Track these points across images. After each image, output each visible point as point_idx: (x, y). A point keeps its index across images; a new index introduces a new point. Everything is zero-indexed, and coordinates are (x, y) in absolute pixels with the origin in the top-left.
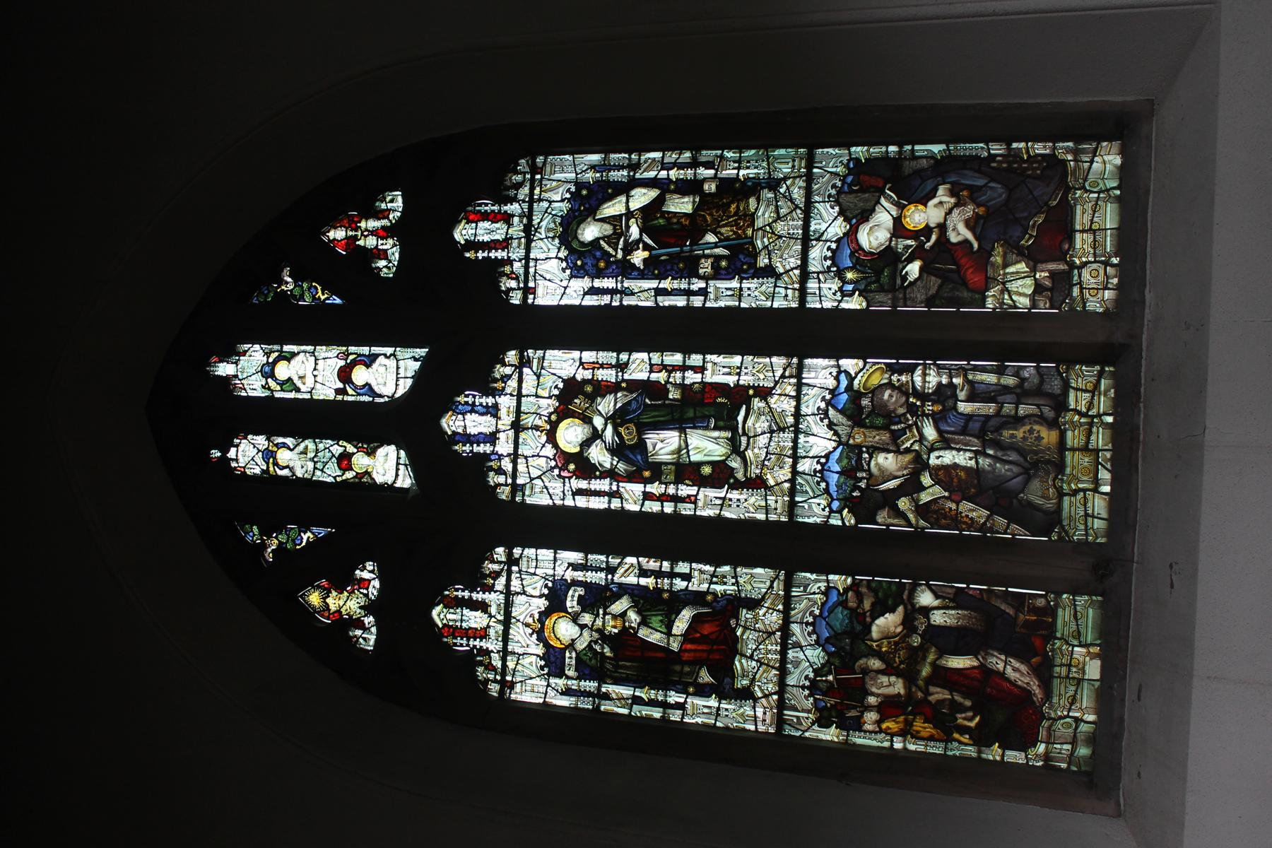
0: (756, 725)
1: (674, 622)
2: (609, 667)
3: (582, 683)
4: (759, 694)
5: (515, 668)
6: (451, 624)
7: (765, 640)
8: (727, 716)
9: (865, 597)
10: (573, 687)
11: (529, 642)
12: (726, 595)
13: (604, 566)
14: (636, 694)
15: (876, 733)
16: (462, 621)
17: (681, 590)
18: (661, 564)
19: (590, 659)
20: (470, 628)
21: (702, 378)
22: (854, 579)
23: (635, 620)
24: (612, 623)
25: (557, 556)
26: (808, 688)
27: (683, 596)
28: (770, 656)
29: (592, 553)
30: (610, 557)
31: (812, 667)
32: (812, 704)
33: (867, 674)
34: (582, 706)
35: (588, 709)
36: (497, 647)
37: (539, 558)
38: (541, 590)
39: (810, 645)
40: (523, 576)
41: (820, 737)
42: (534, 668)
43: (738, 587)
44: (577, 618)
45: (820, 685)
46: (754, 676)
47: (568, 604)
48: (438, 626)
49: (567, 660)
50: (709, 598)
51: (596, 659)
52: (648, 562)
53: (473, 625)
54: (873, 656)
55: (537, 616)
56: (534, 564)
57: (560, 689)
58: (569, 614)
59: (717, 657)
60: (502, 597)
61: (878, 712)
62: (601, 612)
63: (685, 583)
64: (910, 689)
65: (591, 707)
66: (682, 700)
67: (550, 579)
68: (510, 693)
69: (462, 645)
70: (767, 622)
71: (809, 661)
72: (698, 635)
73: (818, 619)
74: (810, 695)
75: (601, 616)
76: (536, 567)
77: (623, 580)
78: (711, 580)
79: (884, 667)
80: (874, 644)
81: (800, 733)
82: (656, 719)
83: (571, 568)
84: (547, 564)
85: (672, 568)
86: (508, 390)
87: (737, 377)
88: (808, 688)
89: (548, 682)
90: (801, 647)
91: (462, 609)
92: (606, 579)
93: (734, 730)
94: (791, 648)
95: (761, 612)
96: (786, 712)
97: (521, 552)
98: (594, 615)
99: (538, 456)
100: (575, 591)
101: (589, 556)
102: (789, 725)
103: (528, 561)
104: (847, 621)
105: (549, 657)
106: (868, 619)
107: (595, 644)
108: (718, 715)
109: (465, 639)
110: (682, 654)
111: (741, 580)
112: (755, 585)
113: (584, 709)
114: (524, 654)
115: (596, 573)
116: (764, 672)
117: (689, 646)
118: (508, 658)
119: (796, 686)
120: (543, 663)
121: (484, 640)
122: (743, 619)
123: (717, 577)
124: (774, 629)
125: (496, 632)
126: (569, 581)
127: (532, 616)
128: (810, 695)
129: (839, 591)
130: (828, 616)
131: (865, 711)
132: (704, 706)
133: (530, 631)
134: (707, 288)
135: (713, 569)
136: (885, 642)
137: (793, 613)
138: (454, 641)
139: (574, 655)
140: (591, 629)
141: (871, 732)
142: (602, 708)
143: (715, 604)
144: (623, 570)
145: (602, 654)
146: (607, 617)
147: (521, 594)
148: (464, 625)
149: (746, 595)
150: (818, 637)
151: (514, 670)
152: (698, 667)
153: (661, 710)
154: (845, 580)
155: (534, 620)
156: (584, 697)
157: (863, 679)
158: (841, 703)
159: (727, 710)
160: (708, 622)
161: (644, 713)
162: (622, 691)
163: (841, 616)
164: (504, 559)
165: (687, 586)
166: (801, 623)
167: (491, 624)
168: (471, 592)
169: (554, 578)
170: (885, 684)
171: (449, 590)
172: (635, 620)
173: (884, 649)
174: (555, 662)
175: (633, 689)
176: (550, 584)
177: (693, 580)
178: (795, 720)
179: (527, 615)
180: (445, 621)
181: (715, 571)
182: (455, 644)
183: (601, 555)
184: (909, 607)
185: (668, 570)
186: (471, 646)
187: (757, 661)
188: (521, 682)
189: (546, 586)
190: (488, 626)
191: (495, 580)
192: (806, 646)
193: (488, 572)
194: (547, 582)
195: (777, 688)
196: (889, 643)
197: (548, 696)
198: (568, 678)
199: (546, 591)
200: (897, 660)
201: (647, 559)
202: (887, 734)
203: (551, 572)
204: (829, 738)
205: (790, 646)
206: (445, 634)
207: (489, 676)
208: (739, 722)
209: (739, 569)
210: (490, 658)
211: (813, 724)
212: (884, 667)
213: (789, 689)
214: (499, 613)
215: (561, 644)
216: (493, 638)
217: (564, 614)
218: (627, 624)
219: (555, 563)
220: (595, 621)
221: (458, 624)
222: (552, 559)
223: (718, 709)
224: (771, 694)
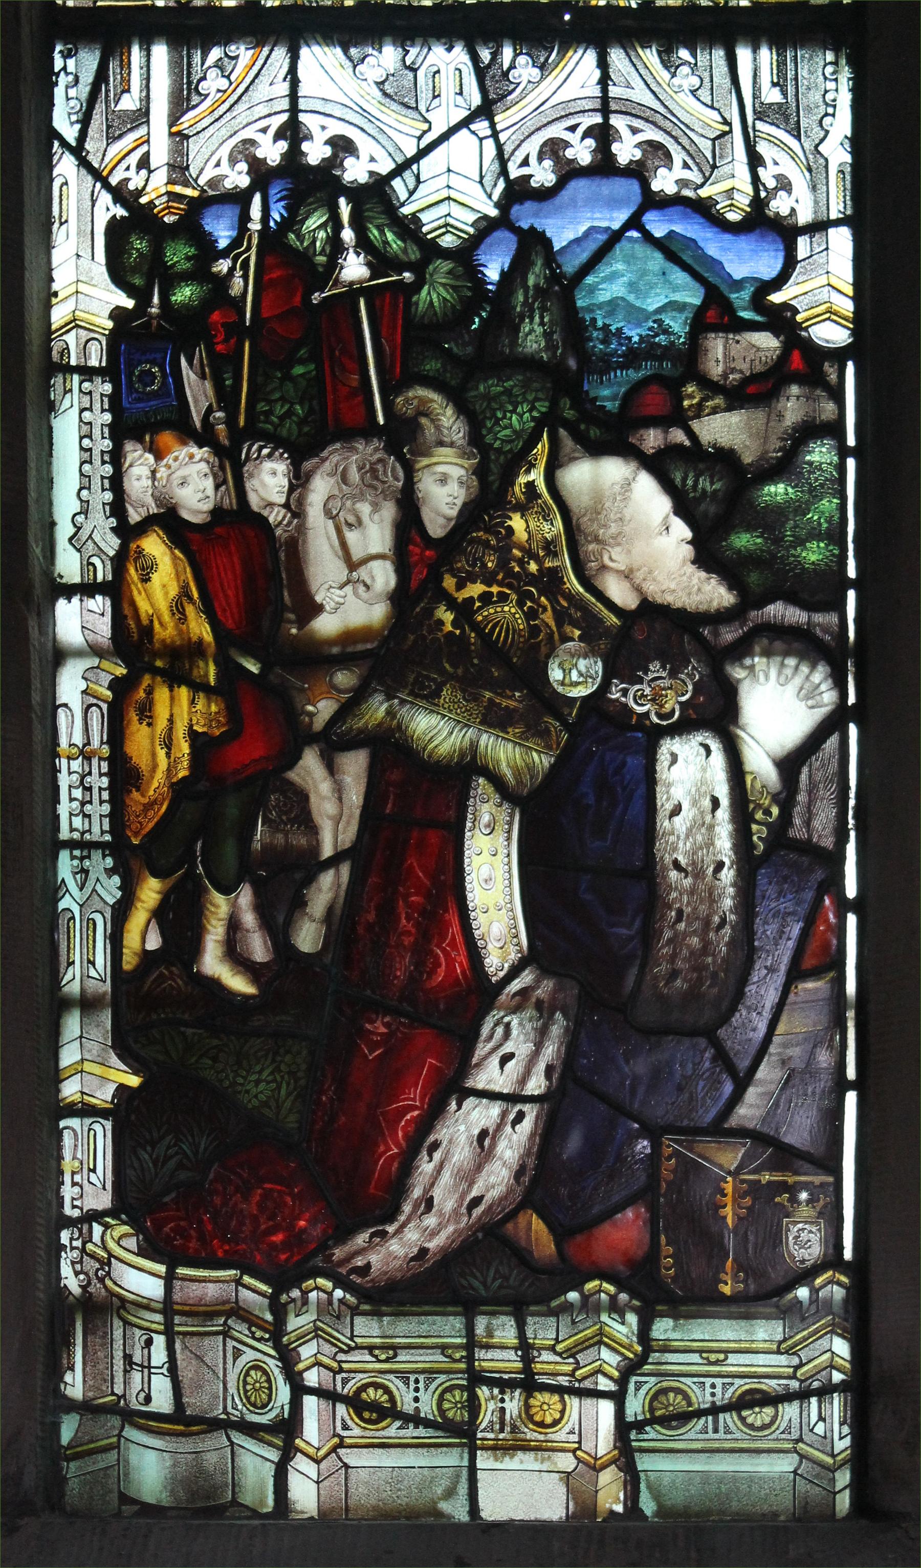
9: (759, 416)
15: (118, 508)
22: (839, 355)
26: (294, 154)
31: (399, 170)
32: (214, 182)
33: (393, 448)
39: (502, 159)
41: (59, 235)
45: (314, 221)
54: (480, 472)
61: (217, 512)
64: (344, 661)
71: (422, 153)
73: (634, 187)
74: (257, 167)
79: (436, 528)
80: (537, 476)
81: (70, 133)
88: (294, 154)
90: (486, 110)
94: (475, 58)
102: (101, 76)
104: (634, 334)
106: (652, 439)
119: (293, 96)
128: (257, 167)
129: (779, 282)
130: (648, 237)
131: (218, 450)
136: (554, 528)
137: (651, 56)
141: (116, 483)
150: (544, 195)
154: (832, 314)
157: (369, 430)
158: (236, 330)
163: (653, 303)
166: (605, 107)
170: (352, 537)
173: (517, 523)
178: (129, 103)
184: (729, 635)
192: (495, 135)
196: (550, 547)
200: (475, 590)
202: (119, 561)
204: (62, 279)
205: (485, 55)
211: (119, 194)
212: (436, 528)
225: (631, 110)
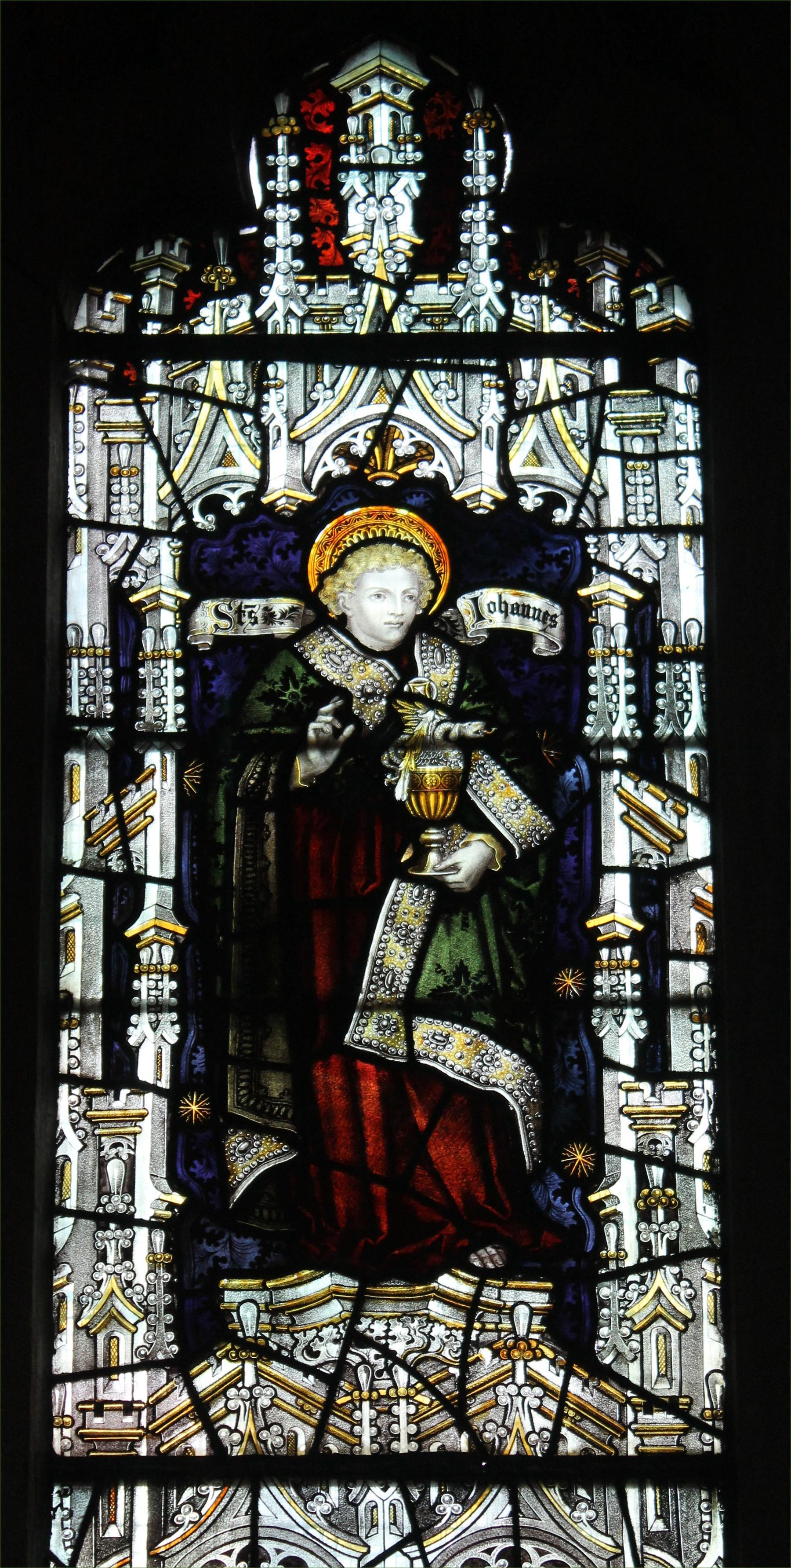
0: (74, 1377)
1: (466, 1021)
2: (252, 770)
3: (171, 671)
4: (204, 1382)
5: (203, 398)
6: (353, 124)
7: (430, 1387)
8: (102, 1257)
10: (148, 635)
11: (312, 446)
12: (600, 1223)
13: (664, 728)
14: (152, 892)
16: (369, 168)
17: (597, 1044)
18: (697, 958)
19: (271, 697)
20: (342, 206)
23: (455, 868)
24: (431, 771)
25: (682, 540)
27: (573, 1050)
28: (366, 1413)
29: (707, 677)
30: (698, 752)
34: (74, 673)
35: (65, 700)
36: (278, 316)
37: (666, 467)
38: (535, 481)
40: (581, 406)
42: (208, 472)
43: (638, 1268)
44: (433, 633)
46: (276, 1356)
47: (489, 595)
48: (336, 69)
49: (257, 604)
50: (579, 1156)
51: (277, 719)
52: (698, 903)
53: (355, 220)
55: (425, 470)
56: (638, 447)
57: (136, 581)
58: (450, 601)
59: (340, 1202)
60: (487, 323)
62: (472, 728)
63: (626, 1055)
65: (75, 710)
66: (145, 1072)
67: (584, 516)
68: (93, 383)
69: (268, 173)
70: (504, 1393)
72: (422, 1122)
75: (455, 729)
76: (625, 456)
77: (613, 808)
78: (653, 1160)
82: (55, 975)
83: (636, 595)
84: (642, 498)
85: (684, 1001)
89: (159, 534)
90: (417, 1537)
91: (415, 168)
92: (608, 743)
93: (49, 1288)
94: (406, 1496)
95: (542, 1368)
96: (142, 1492)
97: (682, 389)
98: (458, 699)
100: (545, 618)
101: (694, 668)
102: (92, 1510)
103: (645, 422)
105: (264, 529)
107: (336, 713)
108: (102, 1220)
109: (295, 185)
110: (335, 1060)
111: (663, 1279)
112: (651, 1334)
113: (64, 682)
114: (263, 430)
115: (630, 700)
116: (299, 1394)
117: (371, 1089)
118: (238, 367)
120: (234, 507)
121: (299, 264)
122: (509, 1297)
123: (669, 1181)
124: (477, 1423)
125: (340, 312)
126: (583, 592)
127: (424, 452)
132: (131, 1165)
133: (360, 448)
135: (699, 1162)
137: (554, 1495)
138: (281, 142)
139: (283, 629)
140: (396, 694)
142: (77, 758)
143: (555, 1180)
144: (652, 804)
145: (301, 745)
146: (454, 754)
147: (508, 402)
148: (353, 181)
149: (605, 1304)
151: (191, 394)
152: (287, 1127)
153: (97, 993)
155: (409, 459)
156: (114, 681)
159: (127, 1254)
160: (480, 1151)
161: (76, 924)
162: (154, 831)
164: (643, 321)
165: (617, 1067)
166: (516, 1533)
167: (371, 291)
168: (493, 197)
169: (588, 531)
171: (487, 107)
172: (455, 868)
174: (242, 554)
175: (170, 873)
176: (561, 516)
177: (646, 1086)
178: (114, 1532)
179: (423, 430)
180: (358, 99)
181: (691, 1172)
182: (267, 148)
183: (707, 715)
185: (674, 987)
186: (269, 214)
187: (341, 1363)
188: (147, 424)
189: (553, 501)
190: (359, 278)
191: (551, 292)
192: (424, 1556)
193: (580, 261)
194: (571, 503)
195: (237, 1451)
197: (99, 535)
198: (186, 611)
199: (530, 502)
201: (709, 898)
203: (613, 515)
205: (416, 1494)
206: (305, 107)
207: (155, 291)
208: (80, 1308)
209: (708, 1267)
210: (230, 293)
213: (242, 1497)
214: (417, 319)
215: (322, 577)
216: (313, 299)
217: (445, 580)
218: (433, 834)
219: (649, 529)
220: (431, 704)
221: (354, 156)
222: (669, 519)
223: (127, 1221)
224: (210, 1427)
225: (537, 1536)
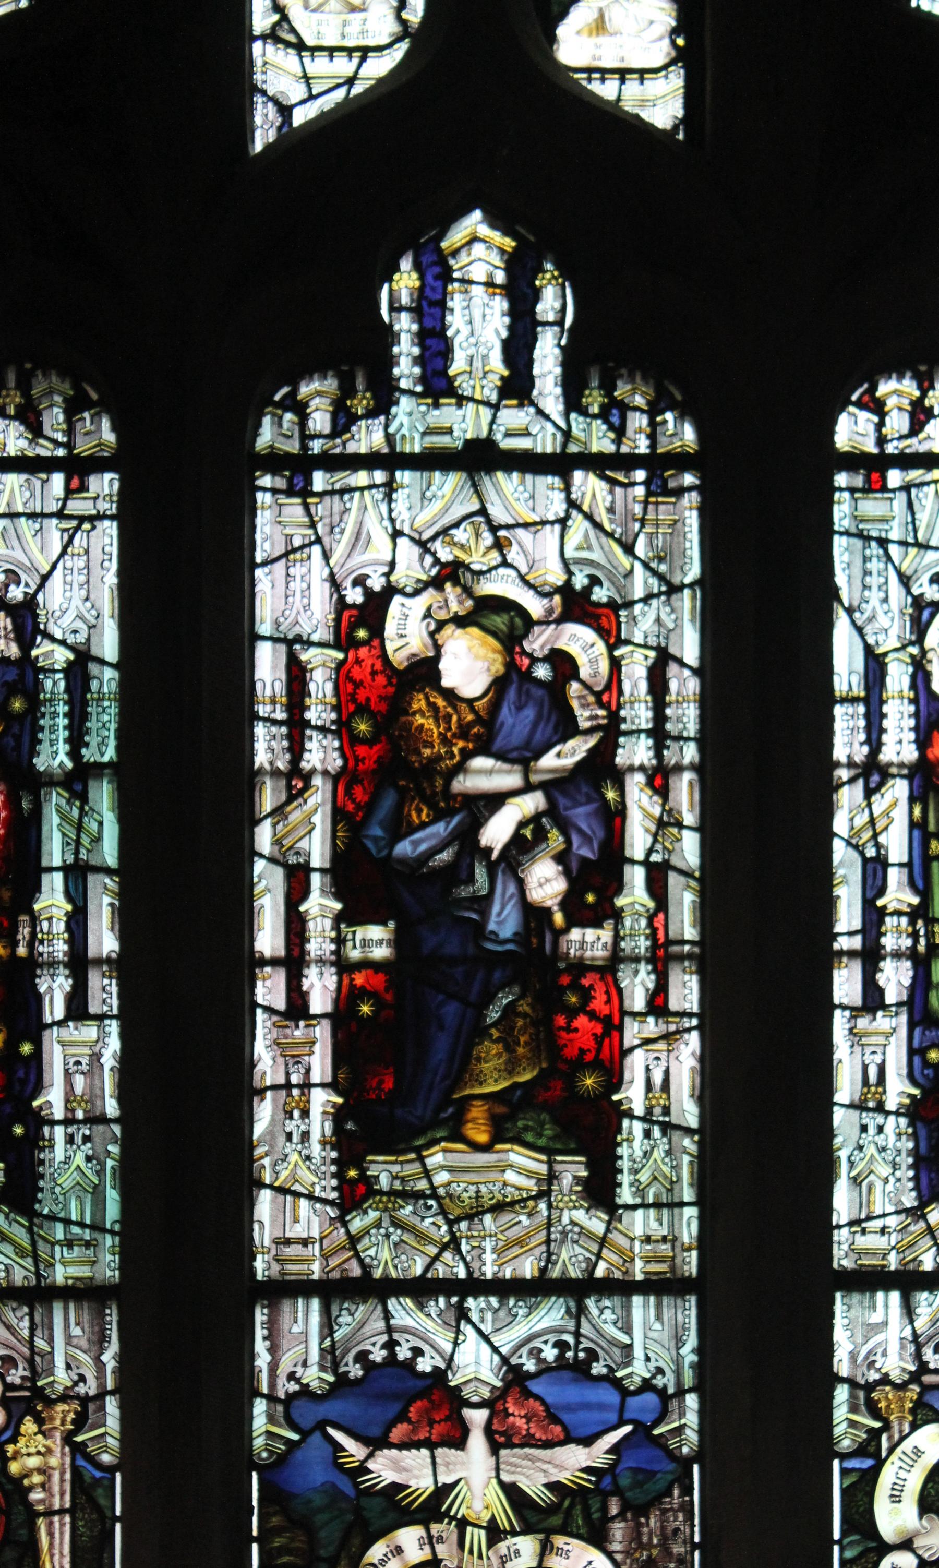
21: (634, 1015)
86: (577, 423)
87: (639, 1110)
99: (396, 534)
134: (884, 1007)
